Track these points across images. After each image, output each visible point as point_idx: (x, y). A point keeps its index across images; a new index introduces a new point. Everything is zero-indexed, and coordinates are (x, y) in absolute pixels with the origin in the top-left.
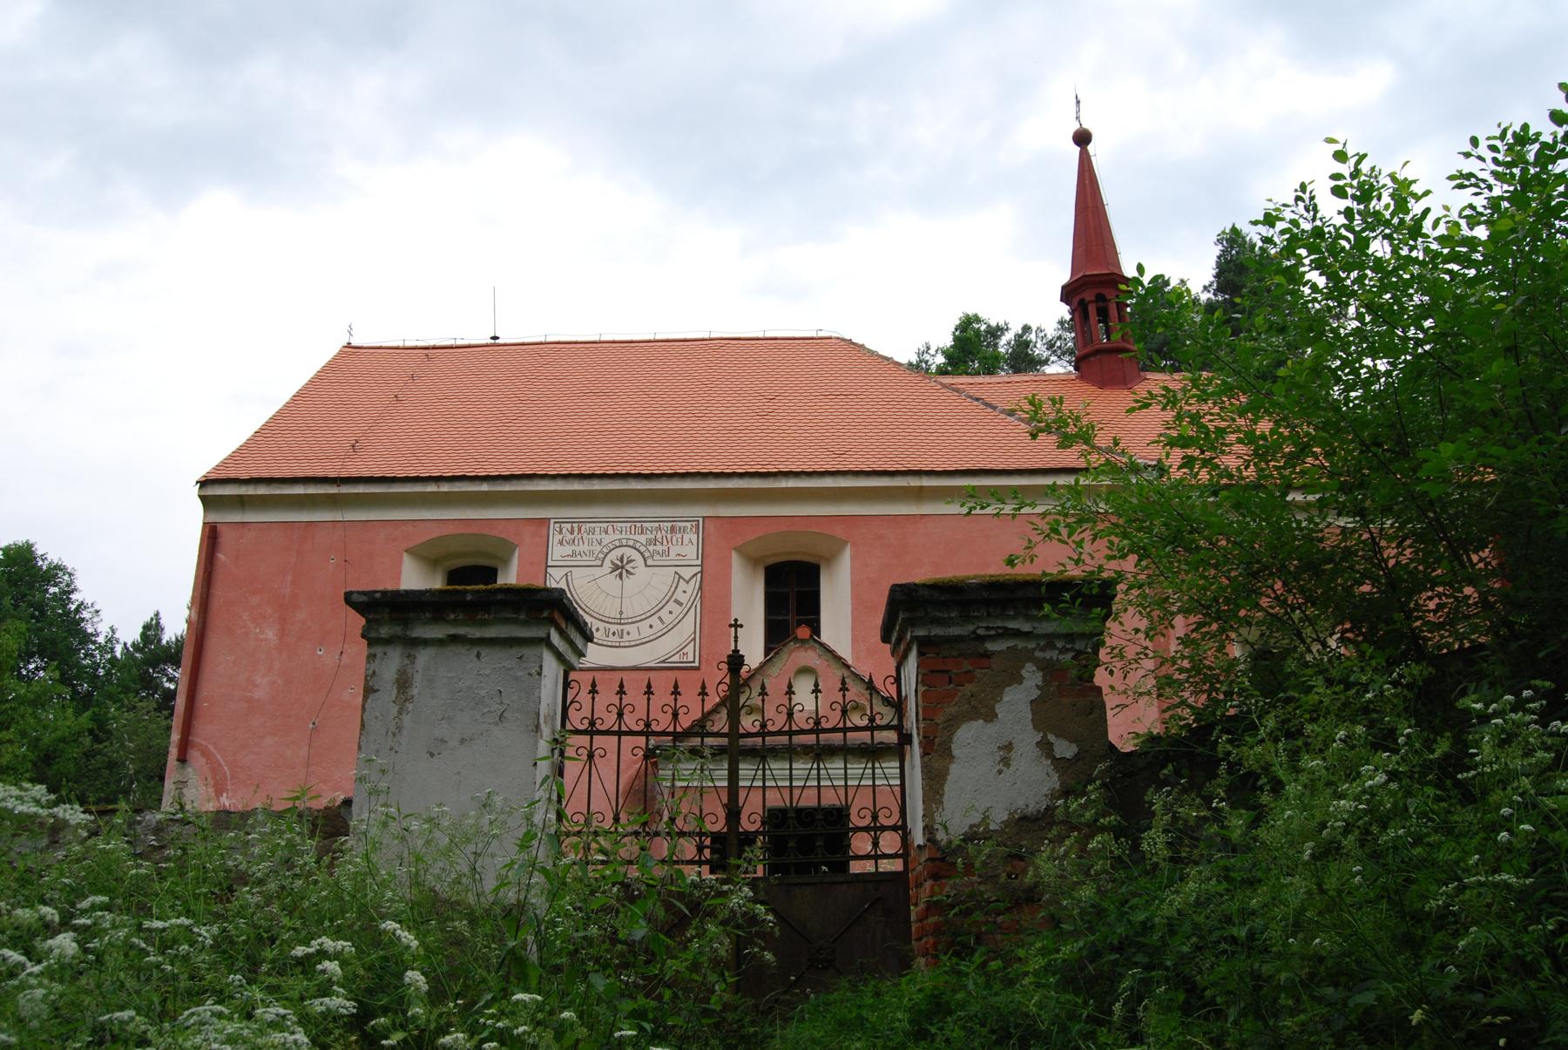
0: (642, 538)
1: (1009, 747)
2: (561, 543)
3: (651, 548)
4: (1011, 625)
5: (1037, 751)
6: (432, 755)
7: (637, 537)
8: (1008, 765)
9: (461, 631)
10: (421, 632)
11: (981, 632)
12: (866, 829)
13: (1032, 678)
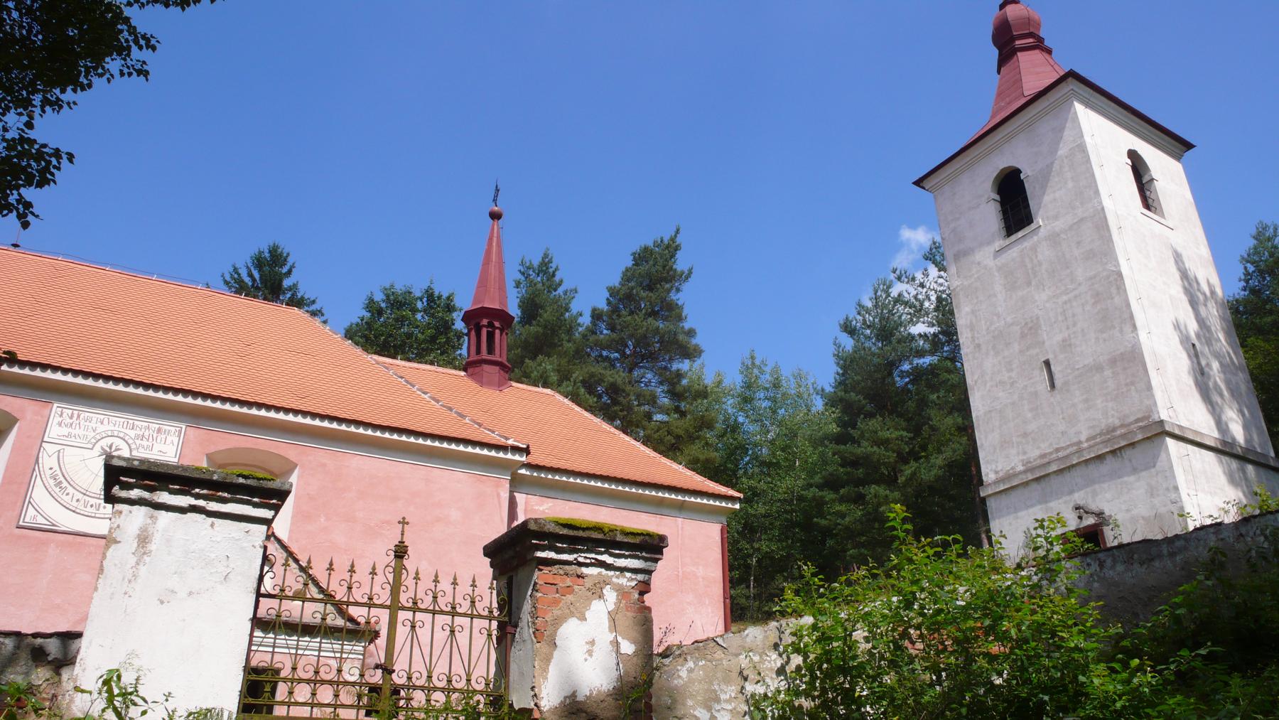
0: (132, 433)
1: (592, 643)
2: (60, 424)
3: (138, 442)
4: (600, 557)
5: (610, 648)
6: (162, 602)
7: (127, 431)
8: (591, 655)
9: (201, 503)
10: (164, 497)
11: (581, 560)
12: (308, 681)
13: (610, 595)
